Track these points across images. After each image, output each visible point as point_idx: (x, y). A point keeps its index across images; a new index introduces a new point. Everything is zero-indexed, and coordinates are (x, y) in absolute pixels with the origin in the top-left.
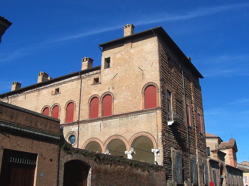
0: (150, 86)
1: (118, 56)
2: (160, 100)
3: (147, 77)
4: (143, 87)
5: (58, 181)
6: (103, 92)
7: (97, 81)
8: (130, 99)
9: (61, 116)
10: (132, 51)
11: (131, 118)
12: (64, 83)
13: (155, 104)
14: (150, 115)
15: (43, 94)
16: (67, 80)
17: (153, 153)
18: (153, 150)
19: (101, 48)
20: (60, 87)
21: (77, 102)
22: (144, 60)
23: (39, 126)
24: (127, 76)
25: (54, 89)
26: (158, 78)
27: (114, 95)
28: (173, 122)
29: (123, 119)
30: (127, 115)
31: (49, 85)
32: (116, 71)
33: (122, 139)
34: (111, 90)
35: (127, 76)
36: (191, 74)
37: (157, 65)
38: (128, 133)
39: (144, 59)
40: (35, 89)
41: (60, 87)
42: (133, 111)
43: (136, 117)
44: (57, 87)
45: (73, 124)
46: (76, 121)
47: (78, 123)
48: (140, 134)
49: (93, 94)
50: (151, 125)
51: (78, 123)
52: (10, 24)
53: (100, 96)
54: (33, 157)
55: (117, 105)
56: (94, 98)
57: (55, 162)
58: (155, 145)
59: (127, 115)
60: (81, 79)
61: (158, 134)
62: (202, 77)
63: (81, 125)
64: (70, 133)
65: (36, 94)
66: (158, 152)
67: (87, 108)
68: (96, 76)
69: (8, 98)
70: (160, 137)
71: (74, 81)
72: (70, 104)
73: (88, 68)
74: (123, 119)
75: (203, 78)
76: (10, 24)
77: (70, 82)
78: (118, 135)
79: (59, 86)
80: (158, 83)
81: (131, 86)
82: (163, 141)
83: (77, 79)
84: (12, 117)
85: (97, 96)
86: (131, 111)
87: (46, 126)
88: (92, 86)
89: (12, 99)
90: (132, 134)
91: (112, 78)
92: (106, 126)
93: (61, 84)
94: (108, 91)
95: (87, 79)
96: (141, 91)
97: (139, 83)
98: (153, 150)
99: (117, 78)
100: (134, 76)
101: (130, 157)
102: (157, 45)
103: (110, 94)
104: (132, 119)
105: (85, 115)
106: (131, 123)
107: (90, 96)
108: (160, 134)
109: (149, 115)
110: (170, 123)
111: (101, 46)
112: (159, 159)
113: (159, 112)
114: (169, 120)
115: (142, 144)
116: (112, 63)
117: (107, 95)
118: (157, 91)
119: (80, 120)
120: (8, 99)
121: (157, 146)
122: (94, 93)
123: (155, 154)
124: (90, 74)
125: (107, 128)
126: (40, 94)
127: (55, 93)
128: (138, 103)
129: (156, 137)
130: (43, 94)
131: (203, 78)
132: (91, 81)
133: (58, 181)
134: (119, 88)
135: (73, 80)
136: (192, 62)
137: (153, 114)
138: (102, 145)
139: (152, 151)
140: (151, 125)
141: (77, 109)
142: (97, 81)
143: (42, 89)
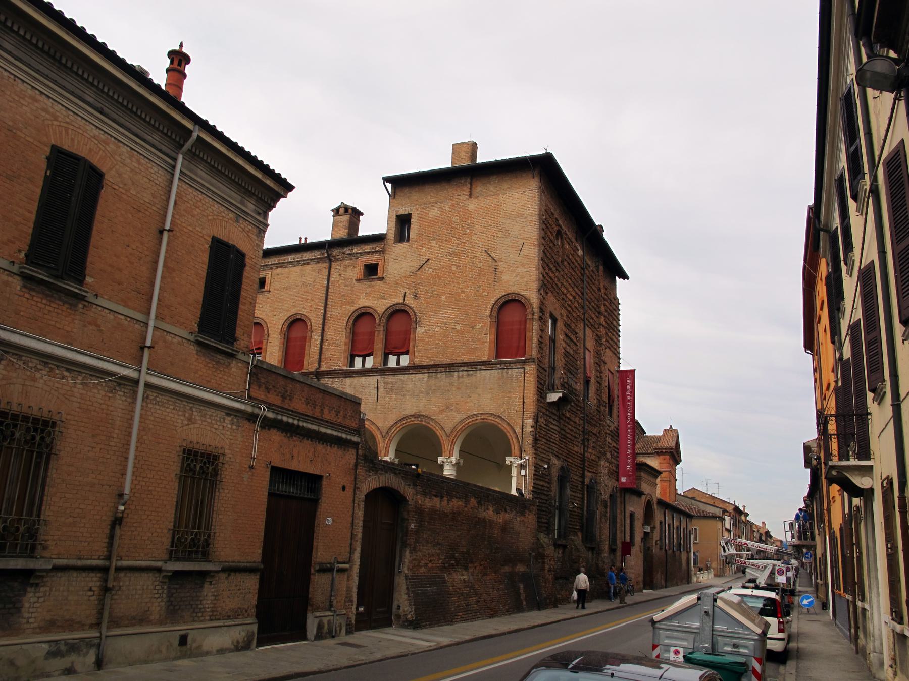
0: (510, 303)
1: (434, 213)
2: (535, 340)
3: (505, 277)
4: (493, 302)
5: (353, 537)
7: (371, 270)
8: (458, 327)
10: (472, 205)
11: (458, 377)
12: (281, 265)
13: (521, 350)
16: (290, 258)
17: (509, 468)
18: (508, 460)
19: (389, 186)
21: (315, 321)
22: (500, 234)
23: (327, 416)
24: (454, 268)
26: (534, 286)
27: (417, 313)
28: (560, 395)
29: (436, 378)
30: (448, 368)
32: (425, 253)
33: (432, 425)
34: (410, 301)
35: (454, 268)
36: (601, 268)
37: (533, 252)
39: (500, 231)
42: (466, 359)
46: (313, 370)
49: (361, 305)
50: (508, 398)
52: (290, 188)
53: (380, 310)
54: (313, 481)
55: (423, 340)
56: (363, 315)
57: (349, 492)
58: (515, 448)
59: (448, 368)
60: (331, 261)
61: (525, 421)
62: (624, 276)
66: (522, 466)
67: (343, 340)
68: (371, 259)
70: (529, 429)
71: (308, 264)
72: (296, 322)
73: (349, 234)
74: (436, 378)
75: (628, 278)
76: (290, 188)
77: (298, 265)
80: (534, 298)
81: (463, 295)
82: (536, 440)
83: (318, 261)
84: (284, 398)
85: (371, 311)
86: (459, 359)
87: (338, 413)
88: (359, 284)
90: (458, 417)
91: (414, 269)
92: (391, 390)
93: (271, 269)
94: (401, 301)
95: (346, 262)
96: (488, 312)
97: (484, 290)
98: (508, 460)
99: (428, 270)
100: (472, 271)
101: (448, 472)
102: (537, 199)
103: (407, 309)
104: (461, 380)
106: (458, 389)
107: (353, 309)
108: (530, 422)
110: (553, 397)
111: (386, 179)
112: (518, 483)
113: (531, 368)
114: (552, 389)
115: (485, 442)
116: (416, 231)
117: (399, 312)
118: (530, 316)
121: (521, 451)
122: (364, 302)
123: (514, 472)
124: (354, 251)
125: (394, 396)
128: (479, 340)
129: (518, 430)
131: (628, 278)
132: (357, 271)
133: (353, 537)
134: (432, 299)
135: (306, 263)
136: (605, 235)
137: (514, 372)
138: (379, 437)
139: (507, 462)
140: (510, 398)
141: (316, 338)
142: (371, 270)
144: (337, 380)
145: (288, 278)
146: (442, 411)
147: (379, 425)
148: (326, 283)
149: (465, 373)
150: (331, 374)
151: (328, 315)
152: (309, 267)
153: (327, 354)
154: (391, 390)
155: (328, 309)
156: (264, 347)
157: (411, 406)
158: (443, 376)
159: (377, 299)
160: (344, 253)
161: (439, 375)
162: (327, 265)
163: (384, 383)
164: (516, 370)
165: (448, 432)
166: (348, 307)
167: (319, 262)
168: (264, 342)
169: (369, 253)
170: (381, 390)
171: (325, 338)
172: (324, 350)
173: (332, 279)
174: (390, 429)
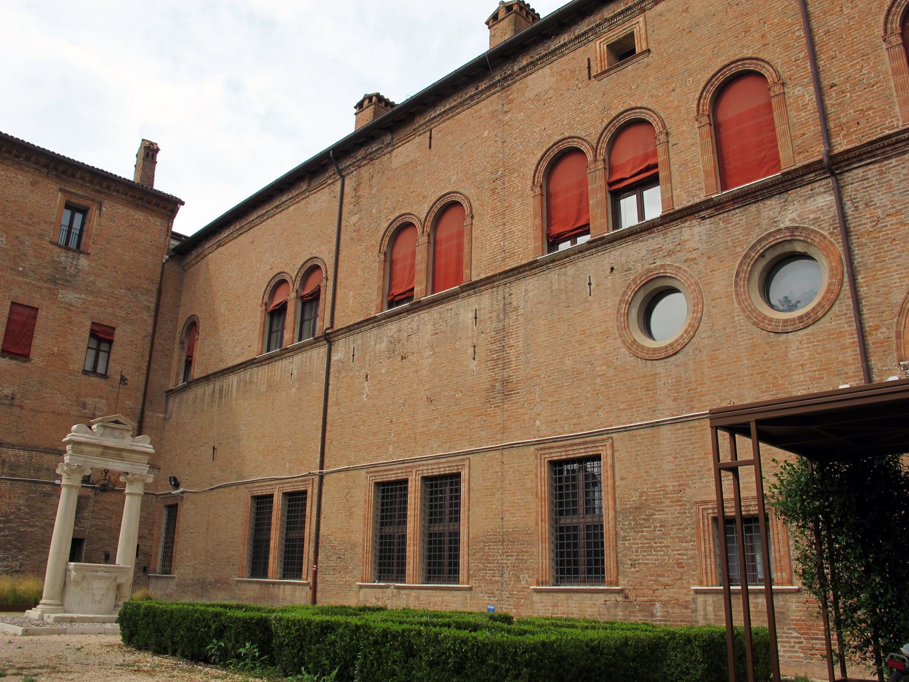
9: (674, 168)
15: (530, 94)
20: (638, 25)
21: (783, 57)
25: (598, 48)
31: (564, 38)
40: (482, 86)
41: (638, 25)
44: (617, 33)
45: (790, 182)
47: (834, 166)
51: (834, 166)
63: (854, 178)
64: (772, 241)
65: (490, 105)
69: (340, 172)
79: (627, 25)
89: (363, 170)
93: (643, 10)
119: (841, 145)
120: (343, 178)
126: (512, 101)
127: (610, 64)
130: (530, 94)
141: (802, 94)
145: (686, 11)
151: (819, 34)
153: (839, 115)
155: (814, 24)
156: (661, 159)
168: (660, 149)
171: (825, 83)
172: (830, 110)
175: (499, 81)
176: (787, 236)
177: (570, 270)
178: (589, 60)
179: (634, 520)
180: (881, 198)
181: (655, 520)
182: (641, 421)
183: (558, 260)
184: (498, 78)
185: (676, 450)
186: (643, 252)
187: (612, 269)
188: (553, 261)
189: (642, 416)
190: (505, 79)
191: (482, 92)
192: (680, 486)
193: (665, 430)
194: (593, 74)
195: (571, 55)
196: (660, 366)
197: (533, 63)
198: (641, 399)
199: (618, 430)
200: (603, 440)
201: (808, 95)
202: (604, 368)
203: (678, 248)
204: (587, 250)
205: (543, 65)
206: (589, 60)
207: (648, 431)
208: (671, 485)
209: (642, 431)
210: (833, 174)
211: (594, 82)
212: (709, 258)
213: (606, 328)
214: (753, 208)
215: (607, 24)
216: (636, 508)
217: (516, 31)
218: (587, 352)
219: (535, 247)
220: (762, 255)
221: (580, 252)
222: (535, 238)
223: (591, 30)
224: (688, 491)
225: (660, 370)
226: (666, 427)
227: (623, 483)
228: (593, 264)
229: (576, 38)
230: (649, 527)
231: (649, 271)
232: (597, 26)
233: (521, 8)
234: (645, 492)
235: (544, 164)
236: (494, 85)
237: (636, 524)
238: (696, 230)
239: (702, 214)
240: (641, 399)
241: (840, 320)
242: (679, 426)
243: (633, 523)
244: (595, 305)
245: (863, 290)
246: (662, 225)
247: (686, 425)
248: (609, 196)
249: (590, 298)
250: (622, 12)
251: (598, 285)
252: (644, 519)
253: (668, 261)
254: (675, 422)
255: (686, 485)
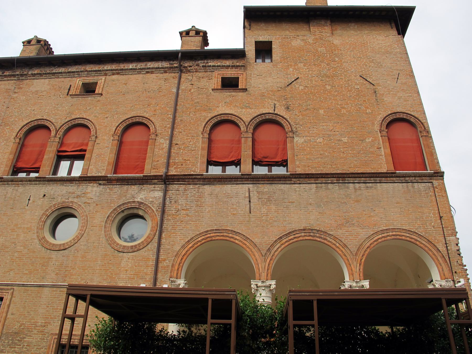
3: (388, 99)
6: (254, 112)
8: (345, 140)
9: (94, 155)
14: (413, 187)
15: (33, 89)
20: (101, 80)
21: (160, 124)
25: (78, 82)
29: (328, 189)
31: (62, 70)
38: (350, 229)
40: (7, 73)
41: (101, 80)
43: (371, 187)
47: (167, 180)
48: (391, 234)
49: (220, 112)
51: (167, 180)
53: (247, 119)
59: (342, 177)
61: (448, 238)
63: (174, 188)
64: (129, 206)
68: (230, 73)
71: (152, 73)
74: (328, 189)
77: (139, 73)
78: (318, 231)
79: (96, 78)
81: (343, 111)
88: (218, 95)
90: (363, 233)
92: (269, 200)
93: (106, 75)
95: (200, 74)
104: (359, 192)
105: (191, 157)
106: (357, 201)
107: (210, 115)
109: (410, 188)
119: (173, 172)
125: (273, 207)
127: (80, 92)
128: (372, 153)
130: (33, 89)
132: (216, 82)
134: (307, 112)
135: (150, 71)
141: (163, 142)
143: (34, 75)
144: (191, 186)
145: (126, 84)
146: (340, 226)
147: (256, 240)
148: (175, 90)
149: (362, 185)
150: (183, 180)
151: (178, 120)
152: (154, 76)
153: (176, 159)
154: (269, 200)
155: (177, 115)
156: (89, 148)
157: (298, 219)
158: (336, 187)
159: (242, 108)
160: (198, 65)
161: (330, 186)
162: (177, 75)
163: (258, 192)
164: (423, 185)
165: (354, 249)
166: (204, 114)
167: (165, 72)
168: (90, 144)
169: (228, 67)
170: (254, 200)
171: (174, 142)
172: (173, 154)
173: (182, 87)
174: (272, 245)
175: (18, 75)
176: (136, 205)
177: (21, 189)
178: (71, 85)
179: (12, 340)
180: (182, 201)
181: (25, 341)
182: (34, 282)
183: (16, 181)
184: (18, 73)
185: (49, 302)
186: (64, 192)
187: (45, 195)
188: (12, 181)
189: (36, 279)
190: (22, 75)
191: (6, 76)
192: (45, 323)
193: (46, 290)
194: (70, 93)
195: (63, 79)
196: (54, 255)
197: (41, 75)
198: (38, 270)
199: (19, 285)
200: (8, 289)
201: (166, 145)
202: (22, 248)
203: (83, 195)
204: (34, 181)
205: (45, 77)
206: (71, 85)
207: (37, 289)
208: (40, 322)
209: (33, 288)
210: (165, 184)
211: (69, 98)
212: (97, 205)
213: (30, 226)
214: (125, 187)
215: (86, 73)
216: (15, 333)
217: (38, 54)
218: (15, 237)
219: (5, 170)
220: (123, 211)
221: (30, 181)
222: (6, 165)
223: (77, 72)
224: (49, 327)
225: (53, 256)
226: (47, 288)
227: (12, 316)
228: (35, 190)
229: (69, 72)
230: (20, 345)
231: (64, 202)
232: (81, 71)
233: (45, 44)
234: (23, 324)
235: (27, 128)
236: (14, 76)
237: (12, 343)
238: (95, 189)
239: (100, 182)
240: (38, 270)
241: (149, 253)
242: (55, 289)
243: (10, 342)
244: (28, 212)
245: (163, 241)
246: (78, 181)
247: (59, 290)
248: (56, 157)
249: (27, 207)
250: (96, 71)
251: (34, 202)
252: (18, 340)
253: (75, 200)
254: (53, 286)
255: (49, 323)
